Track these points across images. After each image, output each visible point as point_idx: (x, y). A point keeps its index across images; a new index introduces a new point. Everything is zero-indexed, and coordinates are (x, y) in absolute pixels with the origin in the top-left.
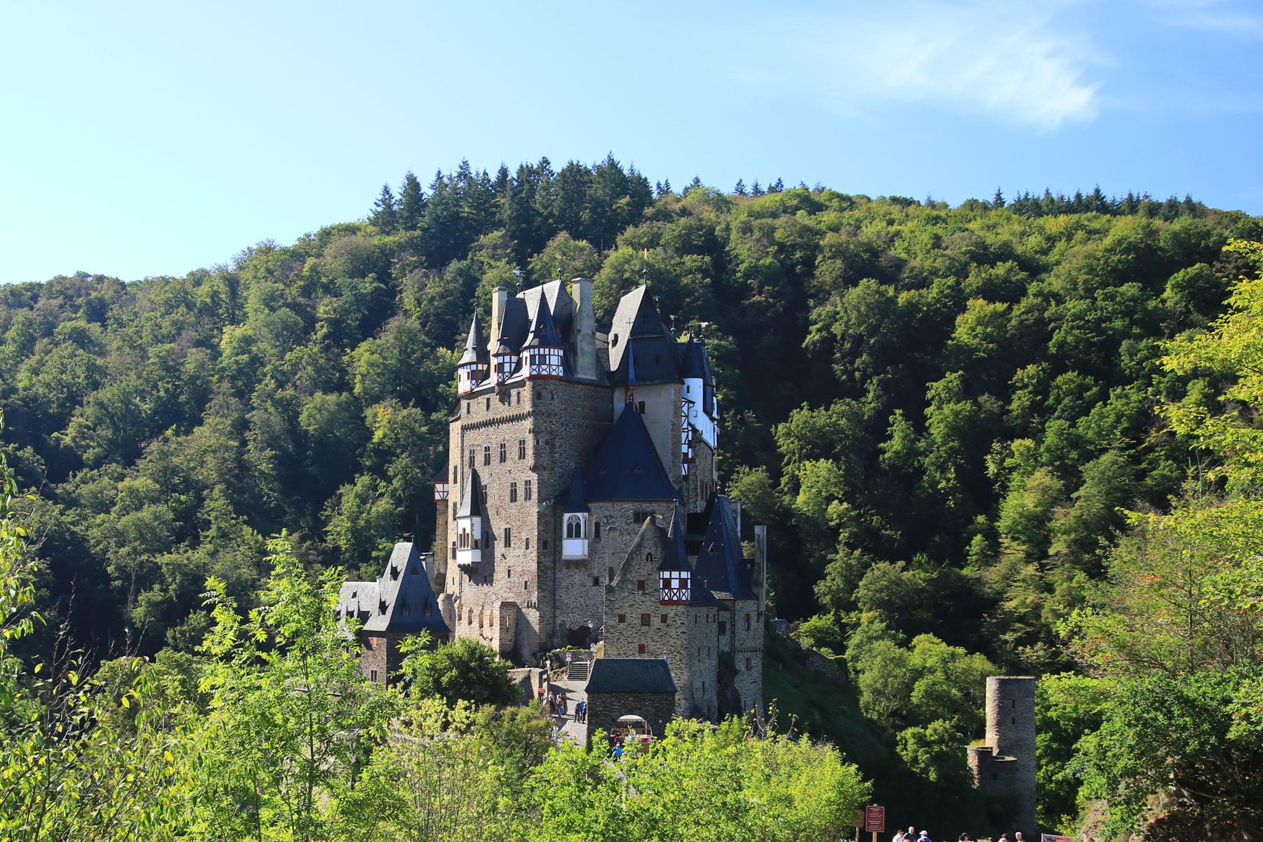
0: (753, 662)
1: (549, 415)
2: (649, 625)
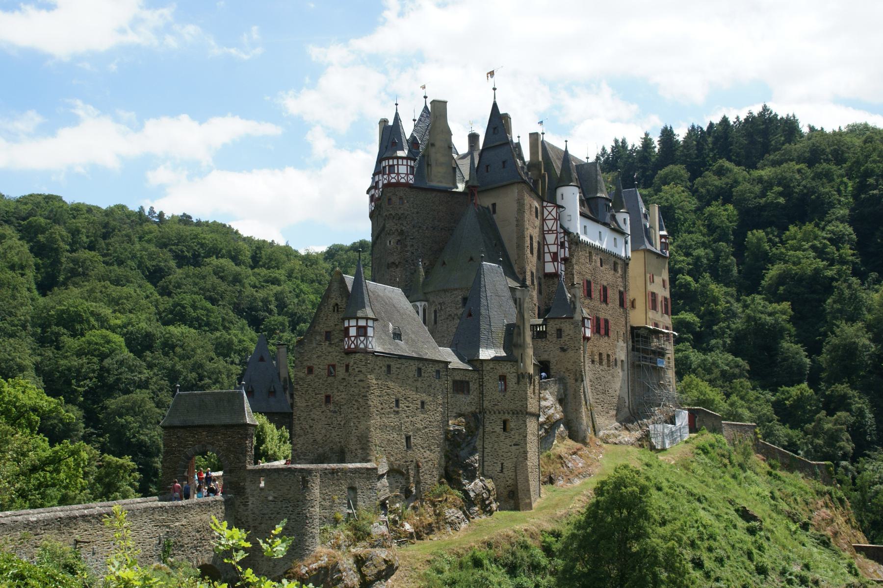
0: (512, 425)
1: (400, 218)
2: (334, 376)
